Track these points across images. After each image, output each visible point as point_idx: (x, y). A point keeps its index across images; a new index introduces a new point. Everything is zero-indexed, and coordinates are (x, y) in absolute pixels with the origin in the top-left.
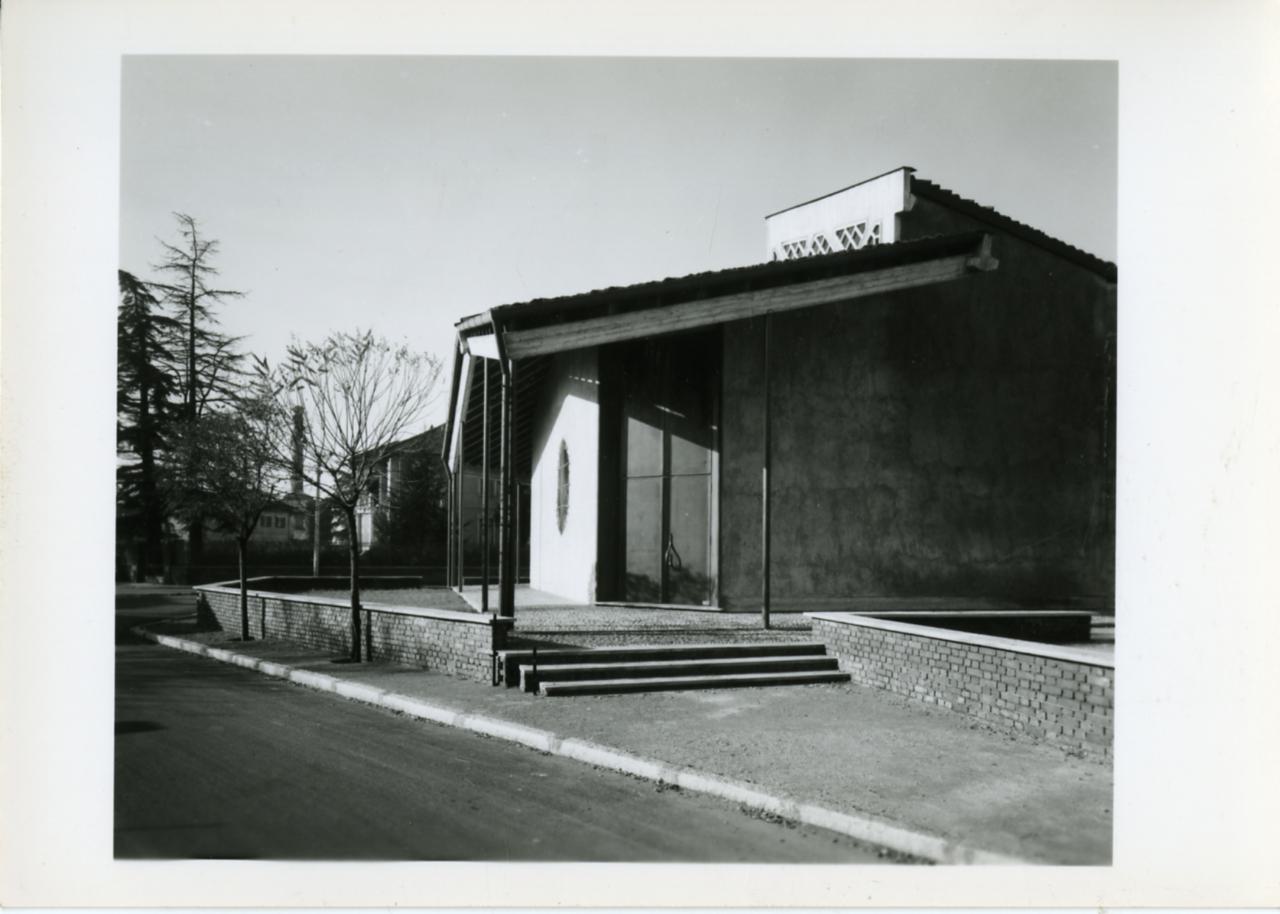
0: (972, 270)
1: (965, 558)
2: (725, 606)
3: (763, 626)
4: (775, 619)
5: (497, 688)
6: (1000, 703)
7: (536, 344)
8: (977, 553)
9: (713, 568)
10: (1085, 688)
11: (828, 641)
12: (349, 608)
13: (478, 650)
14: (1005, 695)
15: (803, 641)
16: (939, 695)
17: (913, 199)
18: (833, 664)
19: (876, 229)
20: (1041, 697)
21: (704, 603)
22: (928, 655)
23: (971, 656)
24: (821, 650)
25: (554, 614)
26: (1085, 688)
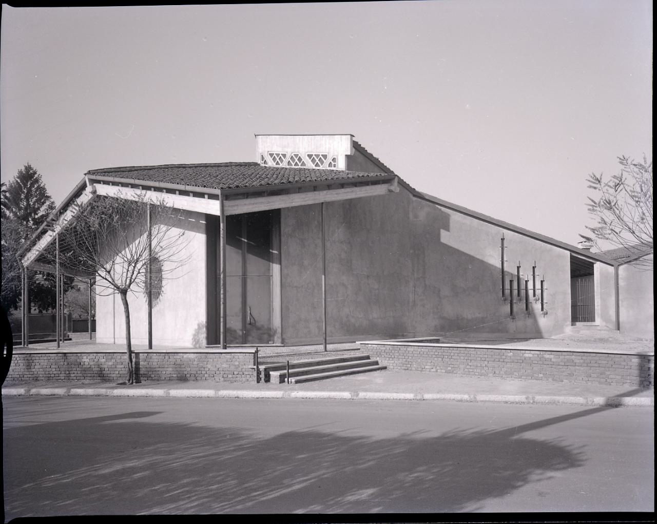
0: (390, 191)
1: (371, 317)
2: (284, 343)
3: (324, 351)
4: (329, 347)
5: (259, 384)
6: (468, 367)
7: (235, 208)
8: (375, 315)
9: (277, 322)
10: (504, 357)
11: (371, 353)
12: (126, 353)
13: (241, 367)
14: (470, 364)
15: (358, 354)
16: (438, 368)
17: (354, 150)
18: (377, 363)
19: (334, 160)
20: (486, 363)
21: (270, 342)
22: (432, 353)
23: (454, 351)
24: (368, 358)
25: (188, 354)
26: (504, 357)
